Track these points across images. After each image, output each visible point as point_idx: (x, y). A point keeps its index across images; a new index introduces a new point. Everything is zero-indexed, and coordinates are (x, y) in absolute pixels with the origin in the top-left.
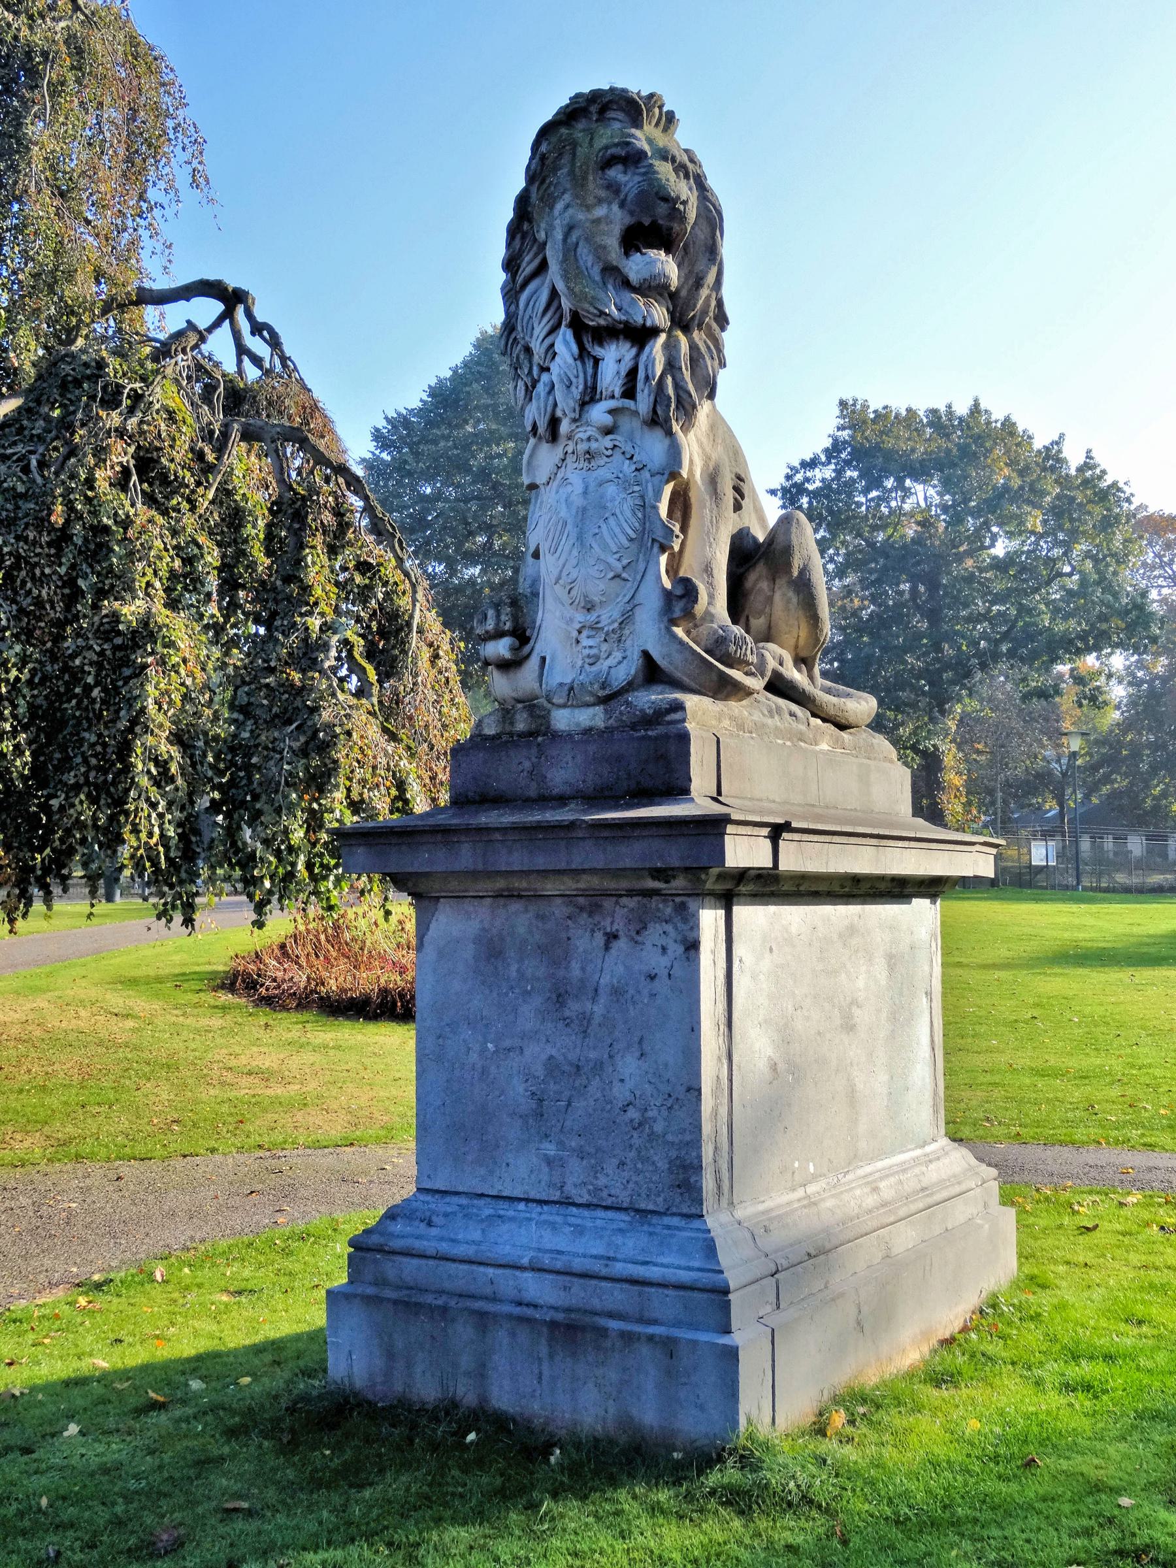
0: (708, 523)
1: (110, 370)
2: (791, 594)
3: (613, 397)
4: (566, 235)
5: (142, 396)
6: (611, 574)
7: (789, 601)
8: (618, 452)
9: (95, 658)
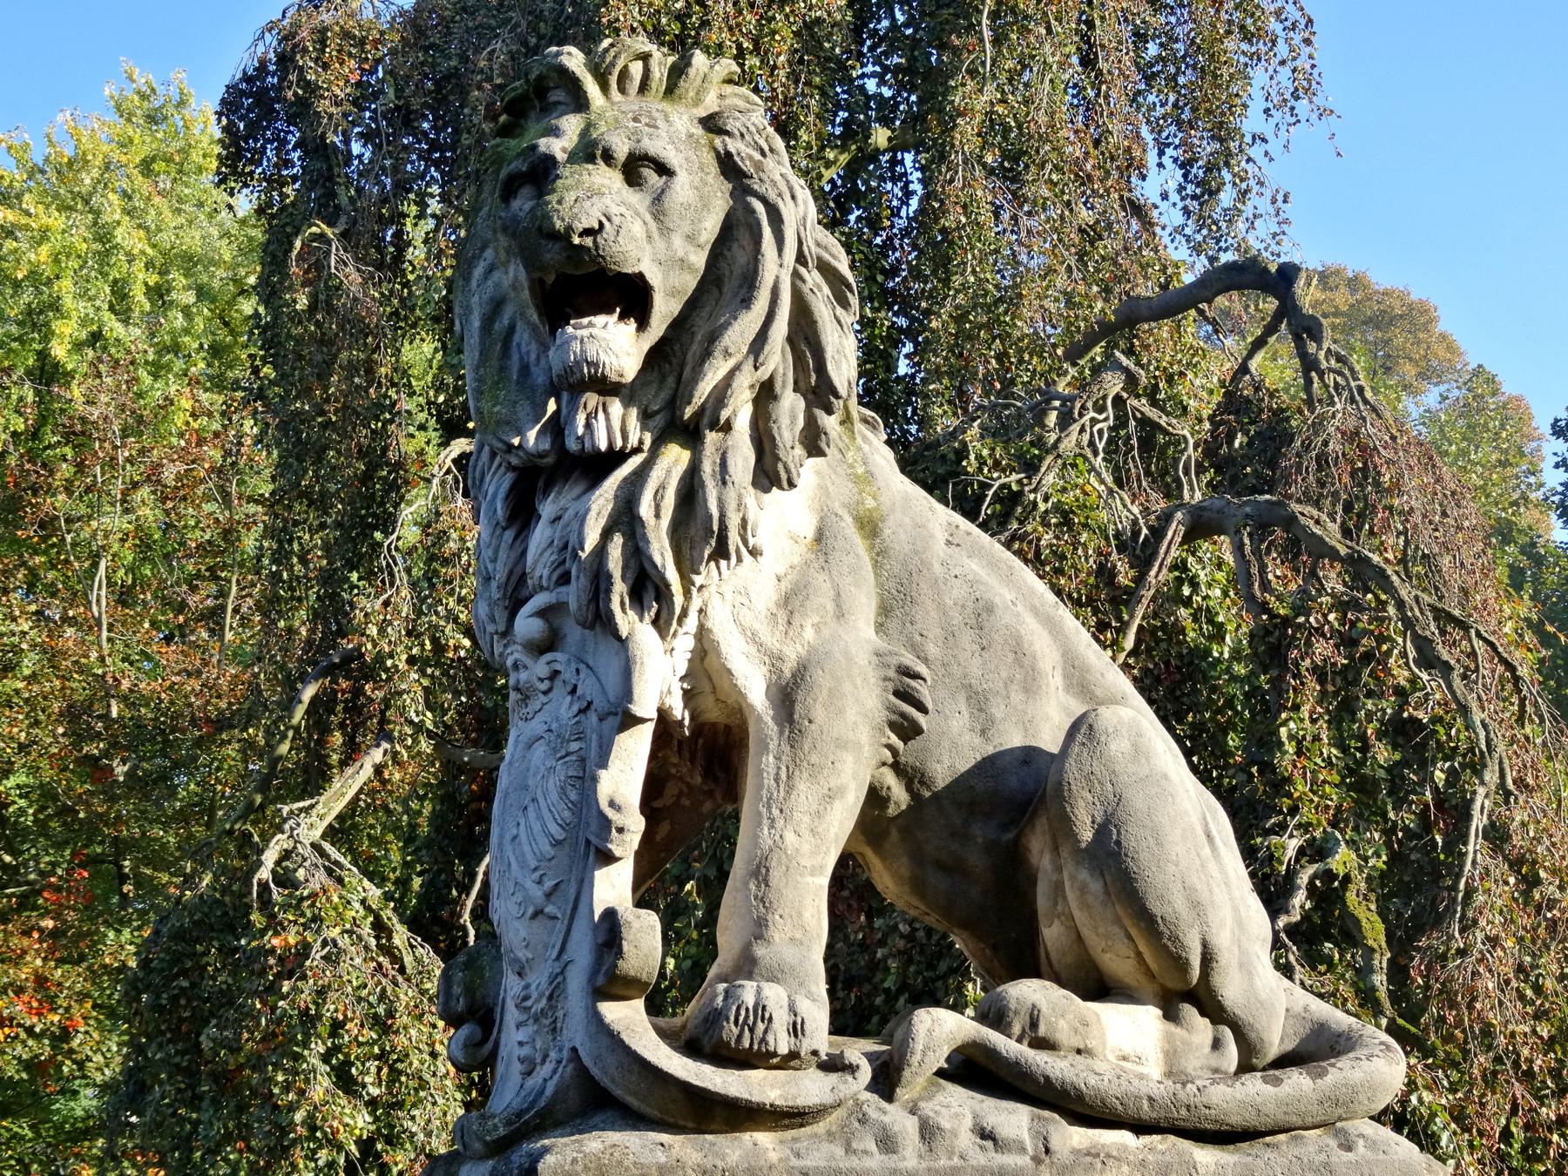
0: (769, 781)
1: (971, 464)
2: (1084, 875)
3: (542, 588)
4: (489, 321)
5: (1021, 493)
6: (531, 910)
7: (1083, 890)
8: (558, 683)
9: (901, 944)
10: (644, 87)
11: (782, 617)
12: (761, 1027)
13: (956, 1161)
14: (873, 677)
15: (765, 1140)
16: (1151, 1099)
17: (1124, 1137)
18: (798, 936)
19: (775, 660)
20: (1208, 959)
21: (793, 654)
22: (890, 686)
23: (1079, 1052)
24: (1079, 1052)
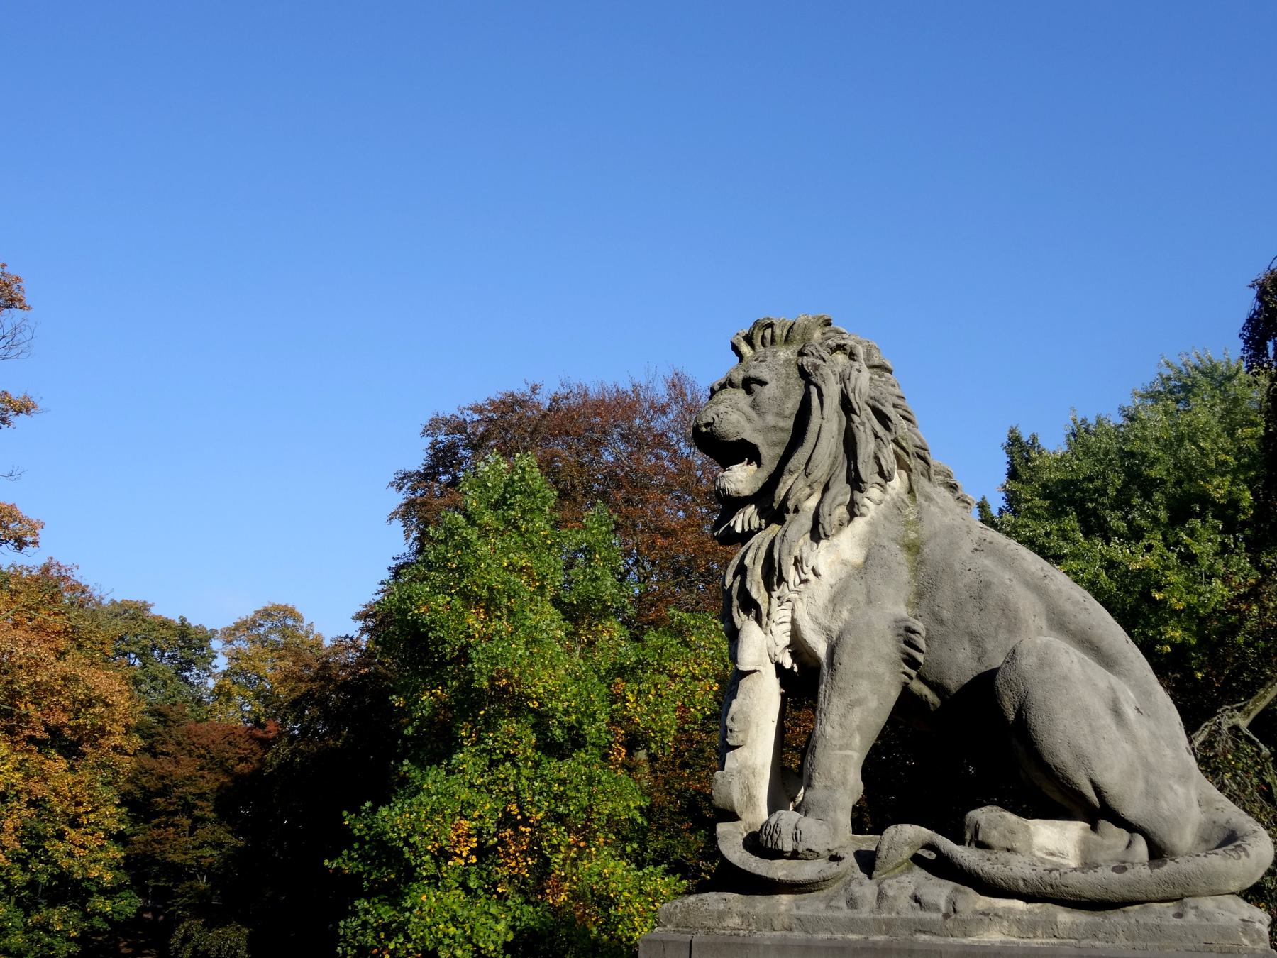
10: (773, 341)
11: (830, 607)
12: (776, 836)
13: (894, 915)
14: (889, 635)
15: (785, 899)
16: (1024, 880)
17: (1019, 905)
18: (829, 784)
19: (827, 631)
20: (1098, 790)
21: (836, 627)
22: (901, 638)
23: (1008, 850)
24: (1008, 850)
